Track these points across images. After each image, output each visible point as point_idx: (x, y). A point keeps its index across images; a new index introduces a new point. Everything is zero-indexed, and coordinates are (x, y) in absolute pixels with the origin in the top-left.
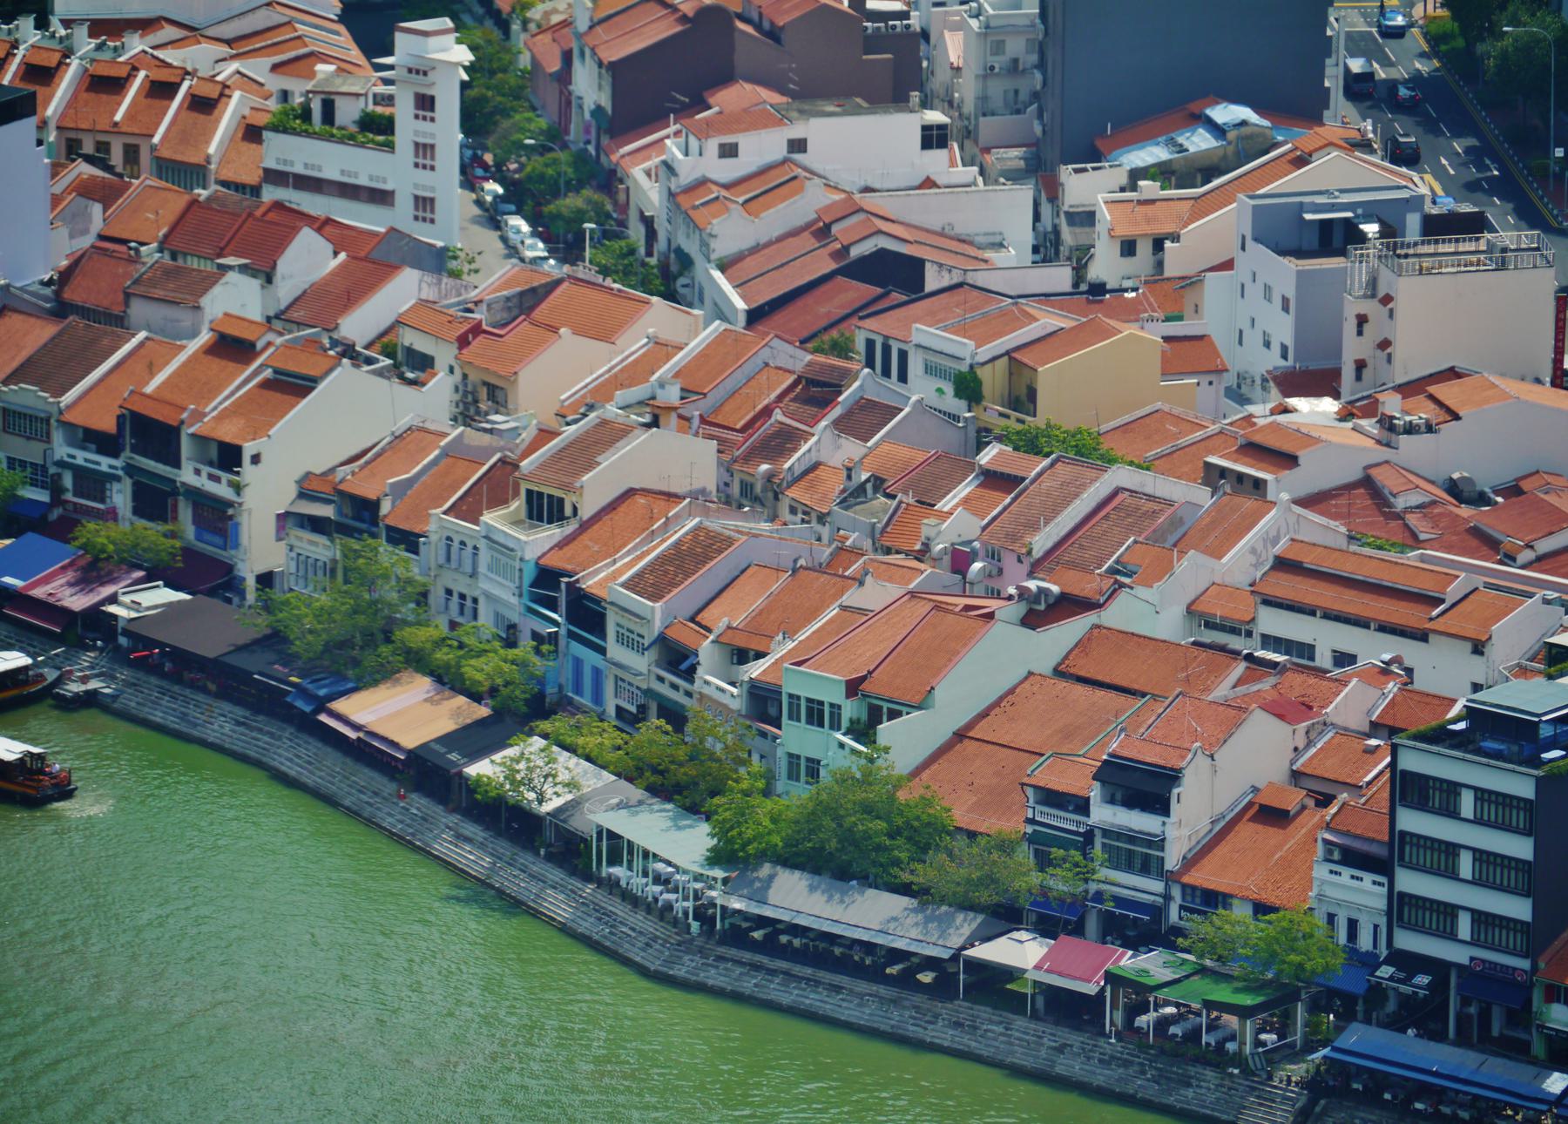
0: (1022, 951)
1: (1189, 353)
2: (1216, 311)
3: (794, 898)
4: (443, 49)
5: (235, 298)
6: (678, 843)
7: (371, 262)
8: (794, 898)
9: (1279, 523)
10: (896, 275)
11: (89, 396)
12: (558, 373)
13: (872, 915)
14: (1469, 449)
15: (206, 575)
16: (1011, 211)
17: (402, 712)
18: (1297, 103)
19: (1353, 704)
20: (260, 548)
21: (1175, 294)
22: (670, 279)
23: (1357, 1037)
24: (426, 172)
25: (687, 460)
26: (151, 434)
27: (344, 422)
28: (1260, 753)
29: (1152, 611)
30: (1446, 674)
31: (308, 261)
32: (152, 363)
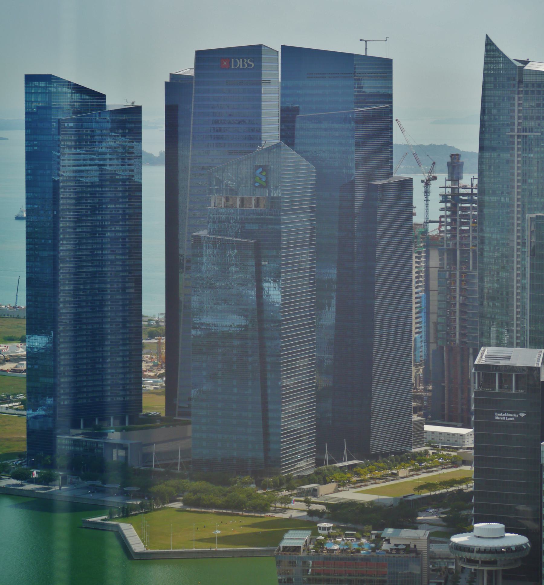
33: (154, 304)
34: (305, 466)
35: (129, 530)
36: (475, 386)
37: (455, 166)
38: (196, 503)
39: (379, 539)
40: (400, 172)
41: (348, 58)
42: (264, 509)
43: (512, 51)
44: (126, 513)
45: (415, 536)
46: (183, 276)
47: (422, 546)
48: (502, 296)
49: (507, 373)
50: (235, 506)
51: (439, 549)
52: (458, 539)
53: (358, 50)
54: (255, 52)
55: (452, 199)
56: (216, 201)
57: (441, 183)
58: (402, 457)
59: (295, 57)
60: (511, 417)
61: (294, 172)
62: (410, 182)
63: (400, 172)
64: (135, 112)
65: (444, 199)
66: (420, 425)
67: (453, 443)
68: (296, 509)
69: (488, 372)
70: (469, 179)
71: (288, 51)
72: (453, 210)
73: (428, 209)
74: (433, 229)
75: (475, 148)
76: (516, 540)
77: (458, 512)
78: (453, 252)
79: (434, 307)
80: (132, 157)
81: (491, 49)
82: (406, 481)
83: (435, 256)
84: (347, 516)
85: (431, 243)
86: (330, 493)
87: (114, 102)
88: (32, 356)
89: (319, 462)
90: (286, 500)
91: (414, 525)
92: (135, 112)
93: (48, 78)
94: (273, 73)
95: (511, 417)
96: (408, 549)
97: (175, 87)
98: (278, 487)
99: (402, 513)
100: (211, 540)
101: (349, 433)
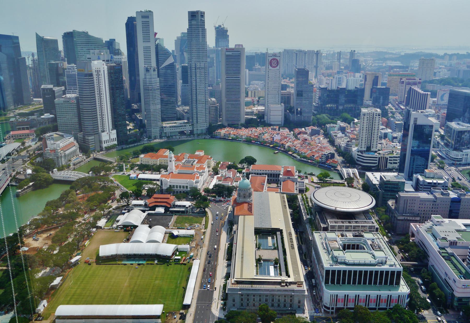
0: (309, 161)
1: (315, 142)
2: (316, 141)
3: (302, 159)
4: (292, 132)
5: (286, 140)
6: (299, 157)
7: (290, 139)
8: (302, 159)
9: (318, 148)
10: (306, 140)
11: (281, 143)
12: (296, 142)
13: (305, 160)
14: (324, 146)
15: (284, 148)
16: (310, 138)
17: (290, 153)
18: (319, 135)
19: (320, 153)
20: (286, 148)
21: (315, 141)
22: (299, 140)
23: (320, 164)
24: (292, 136)
25: (300, 145)
26: (283, 144)
27: (289, 144)
28: (317, 155)
29: (314, 150)
30: (323, 153)
31: (288, 139)
32: (283, 142)
34: (12, 107)
36: (42, 92)
37: (33, 55)
39: (28, 118)
43: (41, 35)
47: (36, 118)
51: (39, 119)
52: (42, 117)
53: (12, 35)
55: (33, 61)
57: (31, 58)
58: (30, 104)
62: (25, 58)
65: (32, 60)
66: (33, 99)
67: (39, 101)
68: (12, 115)
69: (44, 89)
70: (36, 57)
73: (29, 62)
74: (30, 66)
75: (36, 52)
76: (52, 116)
77: (41, 112)
79: (32, 79)
81: (37, 35)
82: (31, 108)
83: (31, 71)
85: (30, 68)
86: (17, 111)
89: (15, 106)
90: (10, 113)
91: (34, 115)
96: (33, 119)
98: (8, 111)
99: (32, 113)
101: (20, 100)
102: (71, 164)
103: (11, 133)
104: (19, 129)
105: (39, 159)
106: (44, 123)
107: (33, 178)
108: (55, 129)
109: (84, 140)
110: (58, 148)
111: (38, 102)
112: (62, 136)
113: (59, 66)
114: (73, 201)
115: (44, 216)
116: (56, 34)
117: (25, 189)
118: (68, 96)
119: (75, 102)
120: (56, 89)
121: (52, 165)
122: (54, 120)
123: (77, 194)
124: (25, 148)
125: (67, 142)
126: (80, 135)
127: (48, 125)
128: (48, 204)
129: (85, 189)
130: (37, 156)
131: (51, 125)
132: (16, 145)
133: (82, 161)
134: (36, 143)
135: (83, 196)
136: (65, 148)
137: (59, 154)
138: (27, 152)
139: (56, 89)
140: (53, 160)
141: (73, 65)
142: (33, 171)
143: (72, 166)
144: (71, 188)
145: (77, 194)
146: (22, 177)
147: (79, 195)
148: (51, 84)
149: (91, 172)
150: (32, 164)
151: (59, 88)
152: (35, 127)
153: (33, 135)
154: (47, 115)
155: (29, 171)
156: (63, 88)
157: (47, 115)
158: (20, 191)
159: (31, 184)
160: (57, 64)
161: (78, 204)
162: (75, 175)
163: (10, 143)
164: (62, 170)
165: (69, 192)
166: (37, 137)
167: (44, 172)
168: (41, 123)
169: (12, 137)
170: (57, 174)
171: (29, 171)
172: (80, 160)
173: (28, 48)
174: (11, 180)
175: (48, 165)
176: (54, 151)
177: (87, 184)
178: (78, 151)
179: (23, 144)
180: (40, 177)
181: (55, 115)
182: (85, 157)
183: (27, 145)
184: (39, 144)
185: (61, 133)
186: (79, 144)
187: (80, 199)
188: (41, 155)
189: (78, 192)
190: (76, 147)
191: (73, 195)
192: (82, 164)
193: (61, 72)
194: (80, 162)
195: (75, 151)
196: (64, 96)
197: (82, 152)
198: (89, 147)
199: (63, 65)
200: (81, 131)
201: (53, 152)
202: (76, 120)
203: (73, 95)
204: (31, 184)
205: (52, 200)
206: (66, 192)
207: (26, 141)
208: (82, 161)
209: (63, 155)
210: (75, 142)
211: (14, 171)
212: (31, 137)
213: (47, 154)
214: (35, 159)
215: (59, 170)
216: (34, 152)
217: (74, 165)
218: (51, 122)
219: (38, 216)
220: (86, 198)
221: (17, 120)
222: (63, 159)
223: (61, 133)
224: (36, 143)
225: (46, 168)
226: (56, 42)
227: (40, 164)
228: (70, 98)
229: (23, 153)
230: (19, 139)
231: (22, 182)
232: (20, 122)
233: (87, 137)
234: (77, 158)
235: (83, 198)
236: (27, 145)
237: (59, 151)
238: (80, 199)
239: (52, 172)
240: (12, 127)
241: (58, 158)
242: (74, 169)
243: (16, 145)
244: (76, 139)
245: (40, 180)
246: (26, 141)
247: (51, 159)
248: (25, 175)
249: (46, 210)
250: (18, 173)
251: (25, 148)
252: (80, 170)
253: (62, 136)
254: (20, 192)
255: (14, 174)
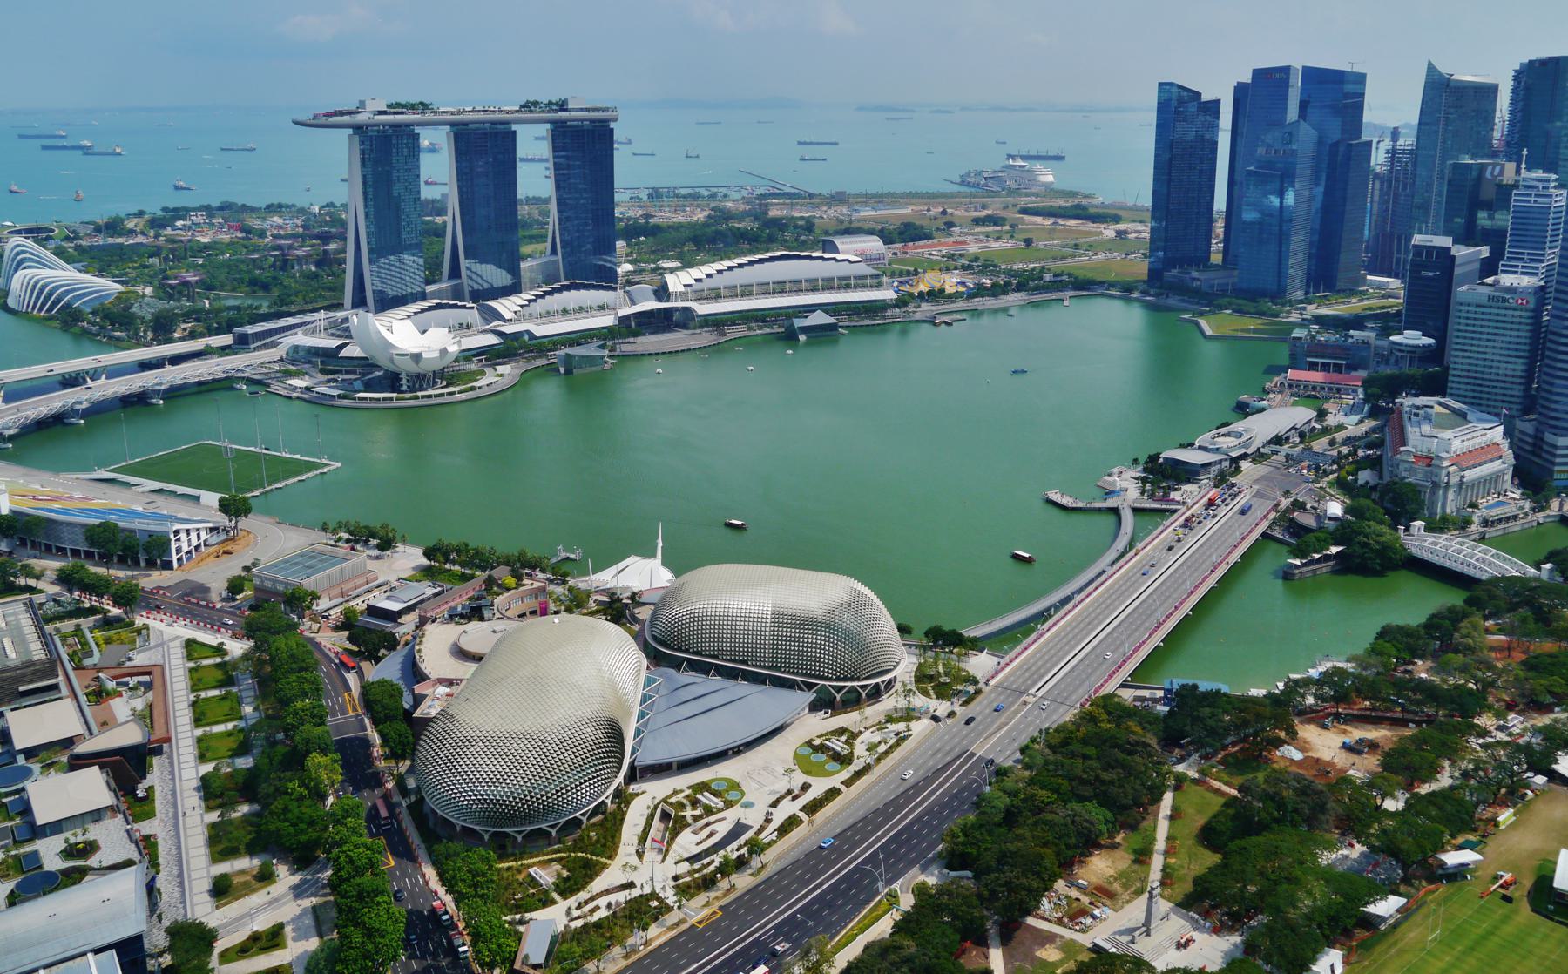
33: (1220, 203)
34: (1299, 294)
35: (1203, 322)
37: (1395, 134)
38: (1238, 311)
39: (1348, 336)
40: (1365, 138)
41: (1341, 73)
42: (1277, 316)
43: (1444, 69)
44: (1202, 314)
45: (1368, 335)
46: (1236, 188)
47: (1372, 341)
48: (1425, 207)
49: (1430, 250)
50: (1261, 314)
51: (1383, 343)
53: (1347, 68)
54: (1286, 70)
55: (1393, 153)
56: (1261, 151)
57: (1387, 143)
58: (1353, 293)
59: (1312, 75)
60: (1430, 274)
61: (1306, 136)
63: (1365, 138)
64: (1216, 103)
67: (1383, 286)
68: (1295, 317)
70: (1407, 141)
71: (1307, 71)
72: (1392, 158)
73: (1378, 158)
74: (1378, 169)
75: (1415, 120)
76: (1432, 341)
78: (1390, 182)
80: (1214, 127)
81: (1430, 64)
82: (1355, 306)
84: (1318, 319)
85: (1377, 176)
86: (1313, 310)
87: (1204, 98)
88: (1153, 231)
89: (1307, 293)
92: (1216, 103)
93: (1171, 84)
94: (1296, 82)
95: (1430, 274)
97: (1241, 91)
98: (1284, 305)
99: (1357, 322)
100: (1248, 331)
101: (1323, 278)
102: (1475, 519)
103: (1291, 374)
104: (1313, 367)
105: (1365, 476)
106: (1392, 360)
107: (1342, 531)
108: (1435, 386)
109: (1534, 445)
110: (1444, 455)
111: (1388, 290)
112: (1463, 415)
113: (1488, 175)
114: (1469, 648)
115: (1365, 669)
116: (1495, 67)
117: (1312, 562)
118: (1507, 280)
119: (1532, 305)
120: (1460, 251)
121: (1411, 507)
122: (1435, 355)
123: (1487, 631)
124: (1326, 431)
125: (1477, 441)
126: (1526, 426)
127: (1406, 369)
128: (1385, 633)
129: (1524, 620)
130: (1360, 465)
131: (1415, 371)
132: (1302, 415)
133: (1515, 518)
134: (1361, 421)
135: (1509, 643)
136: (1465, 460)
137: (1444, 473)
138: (1332, 443)
139: (1460, 251)
140: (1415, 490)
141: (1539, 174)
142: (1347, 511)
143: (1475, 527)
144: (1468, 602)
145: (1487, 631)
146: (1308, 520)
147: (1491, 635)
148: (1446, 233)
149: (1548, 566)
150: (1342, 485)
151: (1472, 249)
152: (1364, 368)
153: (1355, 391)
154: (1413, 338)
155: (1335, 508)
156: (1485, 251)
157: (1413, 338)
158: (1297, 562)
159: (1334, 550)
160: (1482, 167)
161: (1490, 667)
162: (1484, 561)
163: (1280, 405)
164: (1441, 530)
165: (1465, 615)
166: (1366, 401)
167: (1381, 523)
168: (1384, 360)
169: (1290, 386)
170: (1420, 540)
171: (1335, 508)
172: (1508, 510)
173: (1392, 111)
174: (1274, 522)
175: (1402, 502)
176: (1429, 460)
177: (1529, 603)
178: (1508, 477)
179: (1322, 414)
180: (1366, 536)
181: (1442, 338)
182: (1527, 505)
183: (1331, 420)
184: (1370, 424)
185: (1457, 405)
186: (1516, 457)
187: (1491, 649)
188: (1375, 464)
189: (1490, 623)
190: (1502, 464)
191: (1475, 627)
192: (1514, 526)
193: (1488, 193)
194: (1508, 519)
195: (1495, 478)
196: (1490, 280)
197: (1520, 486)
198: (1551, 472)
199: (1502, 173)
200: (1526, 410)
201: (1421, 465)
202: (1519, 366)
203: (1526, 281)
204: (1334, 550)
205: (1401, 623)
206: (1451, 610)
207: (1331, 406)
208: (1515, 518)
209: (1454, 480)
210: (1505, 445)
211: (1287, 494)
212: (1348, 399)
213: (1402, 467)
214: (1354, 473)
215: (1430, 528)
216: (1355, 452)
217: (1485, 522)
218: (1421, 359)
219: (1348, 661)
220: (1519, 656)
221: (1313, 337)
222: (1451, 495)
223: (1457, 405)
224: (1361, 421)
225: (1388, 512)
226: (1490, 91)
227: (1368, 489)
228: (1512, 290)
229: (1319, 445)
230: (1308, 396)
231: (1310, 538)
232: (1320, 344)
233: (1549, 437)
234: (1499, 504)
235: (1507, 649)
236: (1331, 420)
237: (1446, 463)
238: (1491, 649)
239: (1407, 529)
240: (1293, 356)
241: (1435, 485)
242: (1482, 539)
243: (1302, 415)
244: (1507, 433)
245: (1366, 545)
246: (1331, 406)
247: (1410, 484)
248: (1319, 518)
249: (1374, 651)
250: (1298, 505)
251: (1326, 431)
252: (1506, 544)
253: (1463, 416)
254: (1297, 567)
255: (1285, 503)
